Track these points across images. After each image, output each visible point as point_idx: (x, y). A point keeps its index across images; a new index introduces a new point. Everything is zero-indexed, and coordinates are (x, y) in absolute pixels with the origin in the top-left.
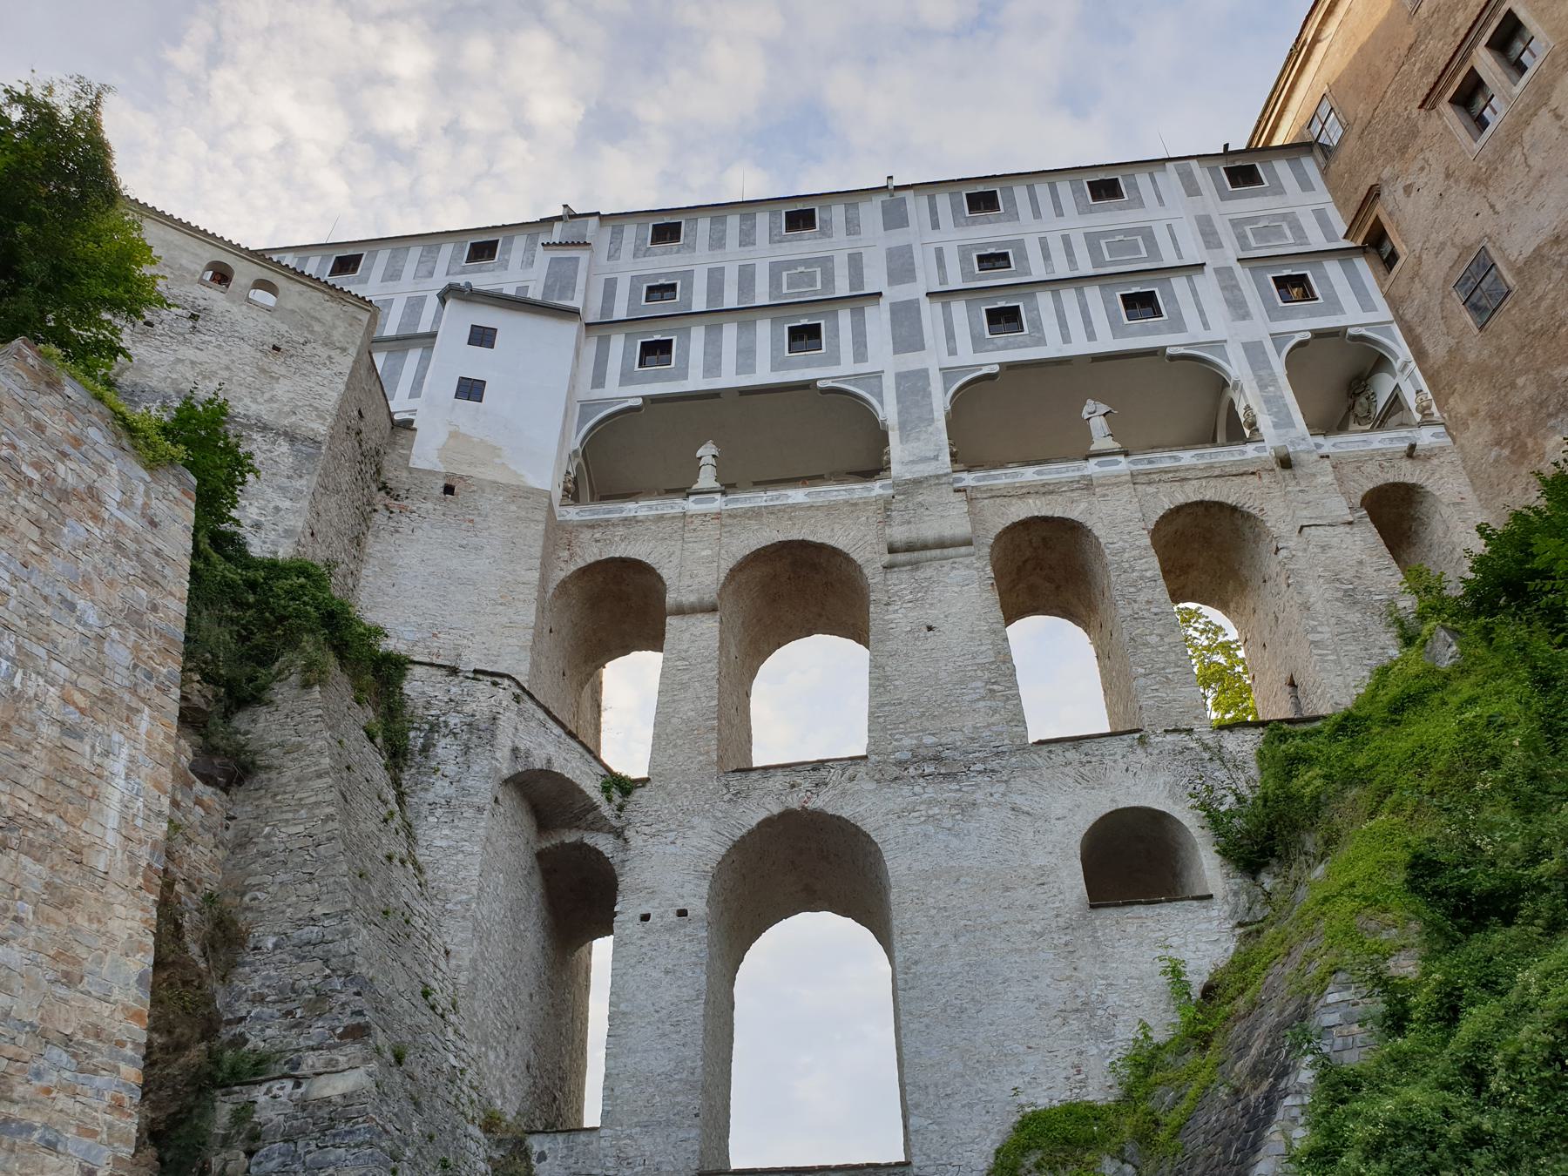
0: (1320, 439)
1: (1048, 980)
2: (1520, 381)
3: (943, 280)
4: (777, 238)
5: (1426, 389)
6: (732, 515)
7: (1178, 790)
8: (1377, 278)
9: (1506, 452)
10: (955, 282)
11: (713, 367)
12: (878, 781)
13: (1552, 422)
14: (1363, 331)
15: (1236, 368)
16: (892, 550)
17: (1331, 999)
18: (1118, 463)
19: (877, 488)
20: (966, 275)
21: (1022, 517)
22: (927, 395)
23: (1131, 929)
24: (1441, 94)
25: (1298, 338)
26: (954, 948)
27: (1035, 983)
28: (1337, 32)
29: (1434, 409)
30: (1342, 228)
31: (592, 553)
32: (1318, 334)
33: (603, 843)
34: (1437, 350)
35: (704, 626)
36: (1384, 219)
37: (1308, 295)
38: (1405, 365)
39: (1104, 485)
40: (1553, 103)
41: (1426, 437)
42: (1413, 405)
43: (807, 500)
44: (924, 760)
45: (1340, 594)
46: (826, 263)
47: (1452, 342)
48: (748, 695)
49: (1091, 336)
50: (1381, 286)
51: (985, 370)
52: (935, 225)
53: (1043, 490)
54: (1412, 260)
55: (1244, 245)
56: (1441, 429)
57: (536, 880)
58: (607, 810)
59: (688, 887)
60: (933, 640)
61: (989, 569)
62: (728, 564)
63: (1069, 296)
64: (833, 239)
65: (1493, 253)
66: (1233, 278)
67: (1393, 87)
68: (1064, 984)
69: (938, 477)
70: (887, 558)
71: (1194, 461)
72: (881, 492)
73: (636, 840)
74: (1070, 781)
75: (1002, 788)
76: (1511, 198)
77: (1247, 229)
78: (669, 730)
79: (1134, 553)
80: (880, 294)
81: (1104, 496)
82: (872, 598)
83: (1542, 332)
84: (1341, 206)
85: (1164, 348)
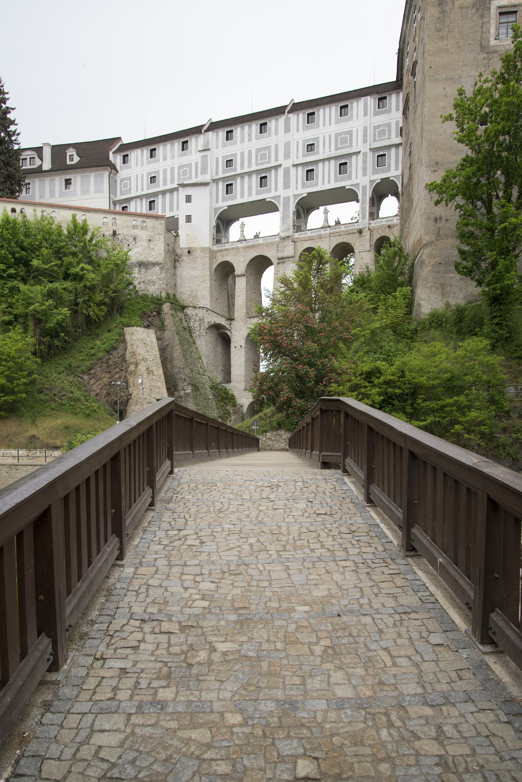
11: (242, 195)
16: (279, 259)
22: (289, 207)
31: (220, 260)
33: (228, 332)
52: (298, 131)
57: (219, 339)
58: (228, 326)
62: (247, 262)
66: (366, 157)
69: (288, 237)
70: (277, 261)
73: (233, 332)
80: (280, 165)
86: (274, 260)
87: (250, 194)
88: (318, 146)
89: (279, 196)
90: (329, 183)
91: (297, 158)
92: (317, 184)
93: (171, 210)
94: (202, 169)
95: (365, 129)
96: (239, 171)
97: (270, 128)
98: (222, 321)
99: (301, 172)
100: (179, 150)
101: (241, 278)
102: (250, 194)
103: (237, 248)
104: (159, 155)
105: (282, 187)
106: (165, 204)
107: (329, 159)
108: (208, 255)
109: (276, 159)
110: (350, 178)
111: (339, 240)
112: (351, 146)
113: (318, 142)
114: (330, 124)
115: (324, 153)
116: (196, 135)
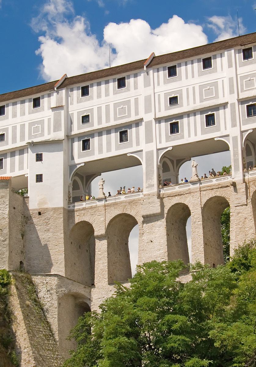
4: (115, 92)
11: (101, 151)
16: (143, 217)
25: (249, 132)
33: (88, 302)
39: (193, 192)
43: (125, 199)
48: (127, 244)
52: (159, 84)
53: (180, 194)
58: (86, 295)
62: (107, 222)
79: (197, 216)
86: (140, 219)
87: (109, 150)
88: (182, 98)
89: (142, 151)
90: (196, 135)
91: (160, 111)
92: (183, 137)
93: (21, 168)
94: (54, 126)
95: (231, 80)
96: (96, 126)
97: (129, 83)
98: (80, 290)
99: (165, 127)
100: (29, 107)
102: (109, 150)
103: (96, 207)
104: (8, 112)
106: (14, 163)
107: (194, 113)
108: (62, 216)
109: (137, 113)
110: (218, 130)
111: (212, 194)
112: (217, 97)
113: (181, 95)
114: (193, 77)
115: (188, 104)
116: (48, 92)
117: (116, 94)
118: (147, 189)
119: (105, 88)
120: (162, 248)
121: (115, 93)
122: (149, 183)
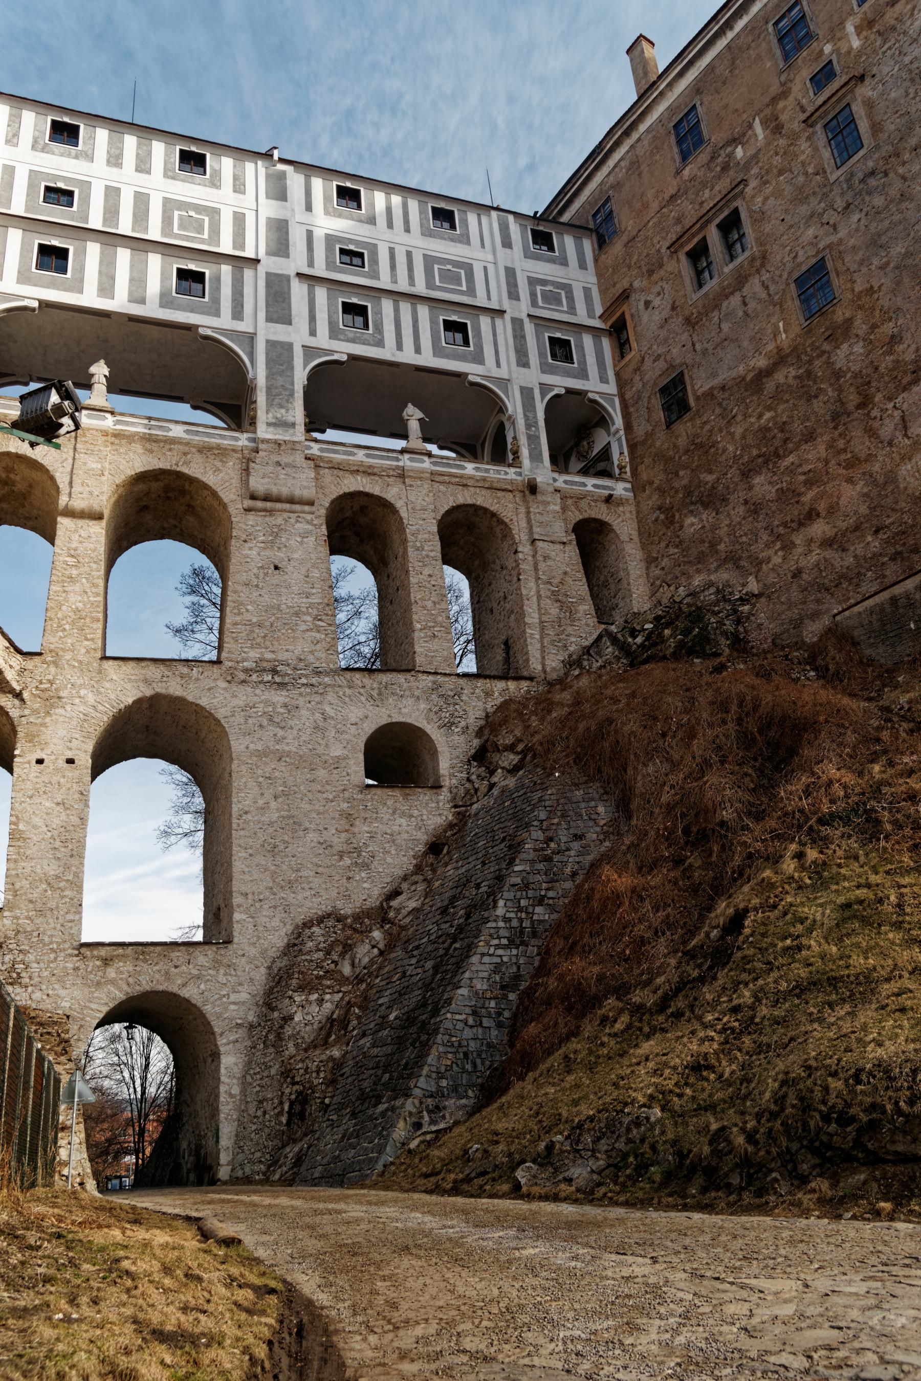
0: (556, 475)
1: (334, 831)
2: (681, 473)
3: (311, 264)
4: (170, 174)
5: (626, 453)
6: (118, 435)
7: (432, 714)
8: (614, 359)
9: (662, 517)
10: (320, 270)
12: (229, 682)
13: (692, 508)
14: (597, 397)
15: (514, 405)
16: (253, 497)
17: (516, 868)
18: (423, 462)
19: (243, 440)
20: (330, 266)
21: (352, 490)
22: (292, 368)
23: (389, 803)
24: (682, 246)
26: (273, 804)
27: (325, 832)
28: (628, 152)
29: (628, 469)
30: (599, 310)
32: (569, 391)
34: (640, 430)
35: (92, 530)
36: (628, 317)
37: (569, 359)
38: (617, 431)
40: (746, 290)
41: (620, 489)
42: (616, 462)
43: (185, 436)
44: (264, 670)
45: (549, 593)
46: (214, 213)
47: (650, 428)
49: (418, 350)
50: (615, 366)
51: (335, 357)
52: (309, 208)
54: (638, 358)
55: (534, 303)
56: (629, 486)
59: (75, 744)
60: (276, 578)
61: (324, 527)
63: (405, 308)
64: (221, 192)
65: (687, 378)
66: (522, 328)
67: (654, 220)
68: (343, 835)
71: (473, 472)
72: (246, 443)
74: (363, 698)
75: (318, 698)
76: (705, 345)
77: (539, 288)
78: (59, 615)
81: (411, 486)
82: (234, 534)
83: (700, 446)
84: (603, 291)
85: (467, 374)
101: (81, 522)
105: (262, 315)
110: (479, 358)
111: (464, 497)
117: (173, 178)
118: (271, 429)
119: (138, 155)
120: (314, 591)
121: (168, 174)
122: (279, 416)
